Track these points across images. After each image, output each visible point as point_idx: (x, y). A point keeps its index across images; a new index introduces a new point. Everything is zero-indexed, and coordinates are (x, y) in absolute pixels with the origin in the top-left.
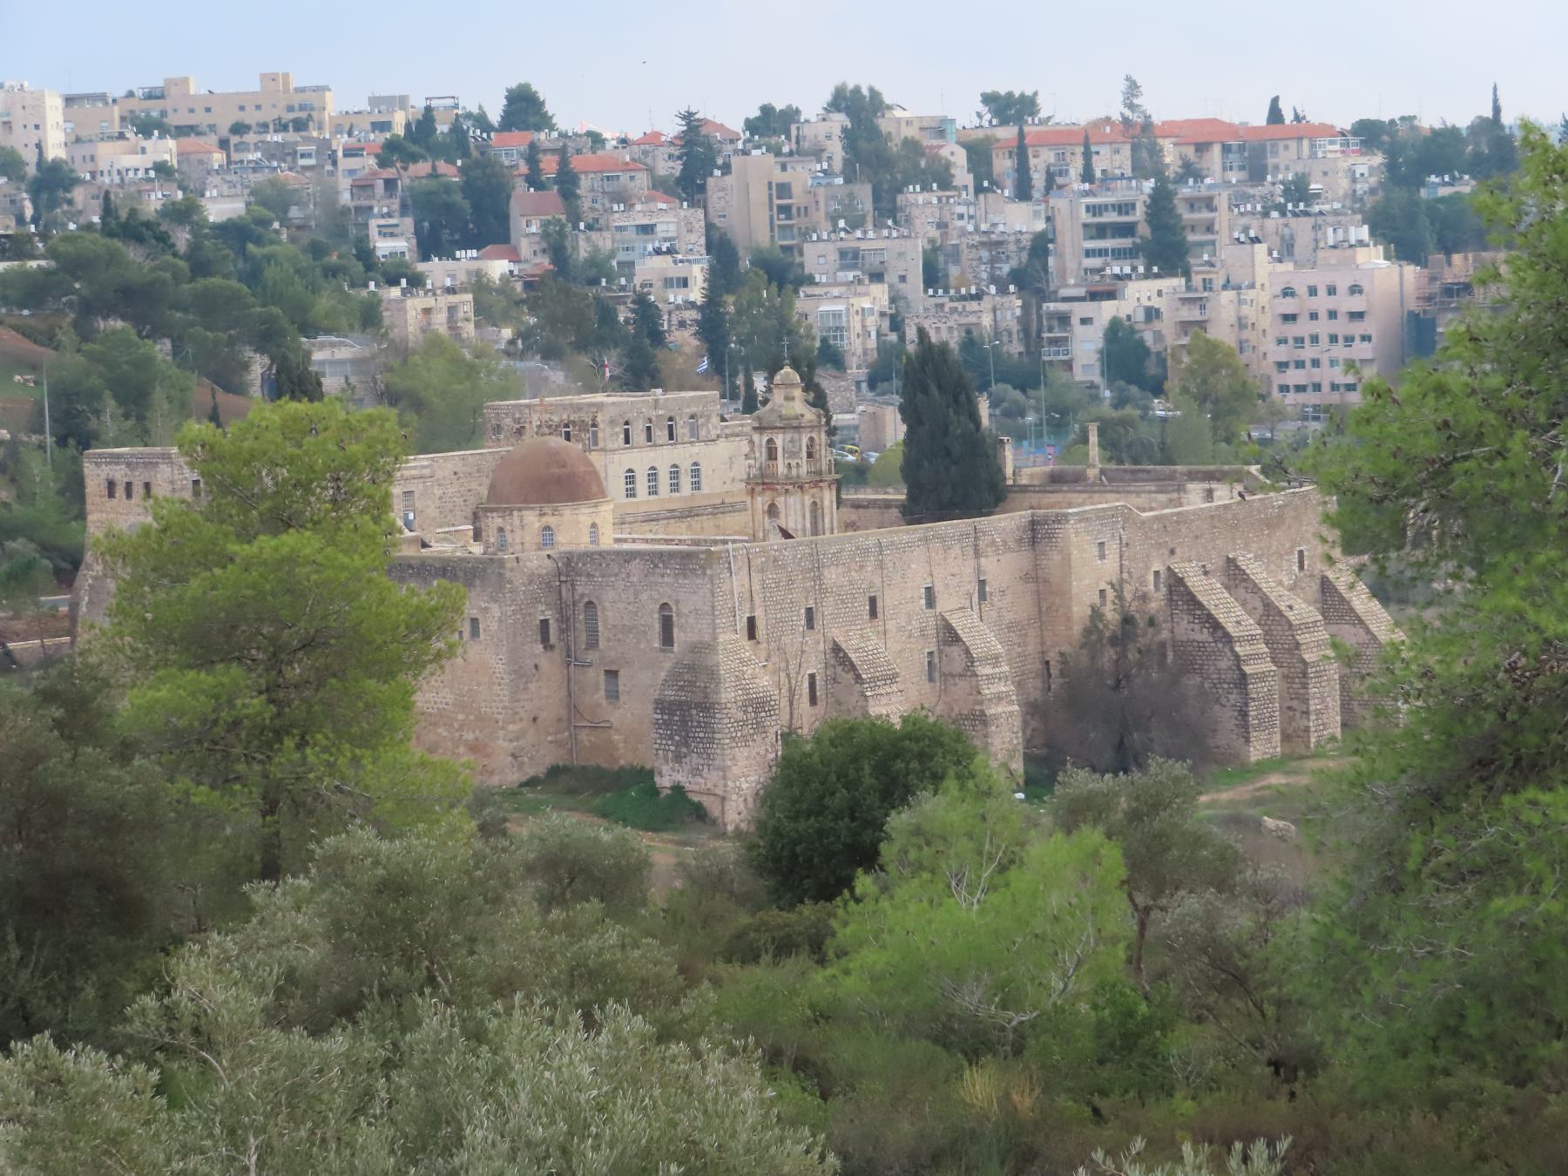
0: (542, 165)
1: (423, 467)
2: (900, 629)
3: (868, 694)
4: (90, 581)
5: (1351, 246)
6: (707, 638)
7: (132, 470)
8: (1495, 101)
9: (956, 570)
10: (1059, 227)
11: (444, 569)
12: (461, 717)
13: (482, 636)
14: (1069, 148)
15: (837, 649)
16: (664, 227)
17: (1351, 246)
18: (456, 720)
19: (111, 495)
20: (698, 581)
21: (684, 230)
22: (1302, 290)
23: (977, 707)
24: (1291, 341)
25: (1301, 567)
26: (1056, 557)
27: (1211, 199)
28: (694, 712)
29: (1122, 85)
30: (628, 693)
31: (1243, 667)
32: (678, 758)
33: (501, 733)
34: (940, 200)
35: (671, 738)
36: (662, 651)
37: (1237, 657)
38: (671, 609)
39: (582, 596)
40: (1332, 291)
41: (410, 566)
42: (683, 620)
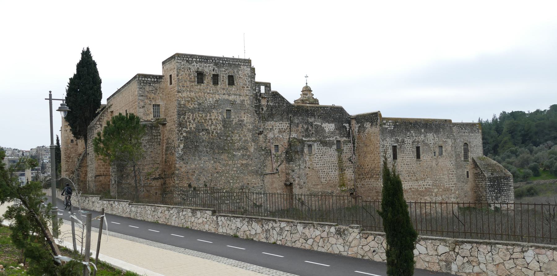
4: (184, 134)
7: (218, 67)
12: (436, 190)
28: (502, 180)
35: (494, 191)
41: (411, 124)
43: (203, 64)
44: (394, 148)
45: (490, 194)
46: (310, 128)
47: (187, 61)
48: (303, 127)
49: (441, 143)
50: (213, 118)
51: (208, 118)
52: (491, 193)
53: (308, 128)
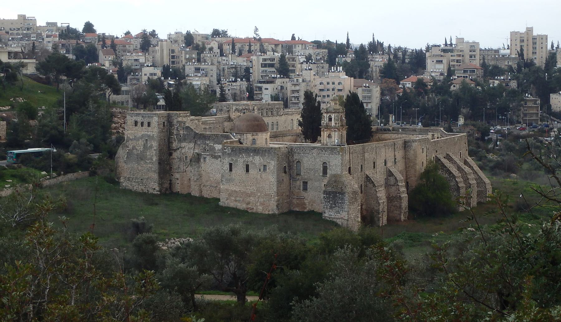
0: (106, 42)
1: (214, 120)
2: (379, 172)
3: (377, 190)
4: (127, 151)
5: (338, 72)
6: (339, 173)
8: (348, 37)
9: (390, 155)
10: (254, 64)
11: (255, 150)
13: (268, 170)
14: (245, 44)
15: (367, 177)
16: (142, 60)
17: (338, 72)
18: (257, 195)
19: (136, 125)
20: (337, 156)
21: (147, 61)
22: (325, 83)
23: (398, 195)
24: (322, 96)
25: (460, 157)
26: (412, 152)
27: (294, 58)
29: (254, 28)
30: (311, 188)
31: (459, 185)
32: (331, 208)
33: (273, 199)
34: (213, 56)
36: (323, 176)
37: (457, 182)
38: (327, 164)
39: (296, 159)
40: (333, 83)
41: (244, 149)
42: (331, 167)
43: (137, 117)
44: (231, 165)
45: (325, 204)
46: (207, 147)
47: (131, 116)
48: (202, 146)
49: (265, 163)
50: (140, 143)
51: (138, 143)
52: (327, 203)
53: (205, 147)
